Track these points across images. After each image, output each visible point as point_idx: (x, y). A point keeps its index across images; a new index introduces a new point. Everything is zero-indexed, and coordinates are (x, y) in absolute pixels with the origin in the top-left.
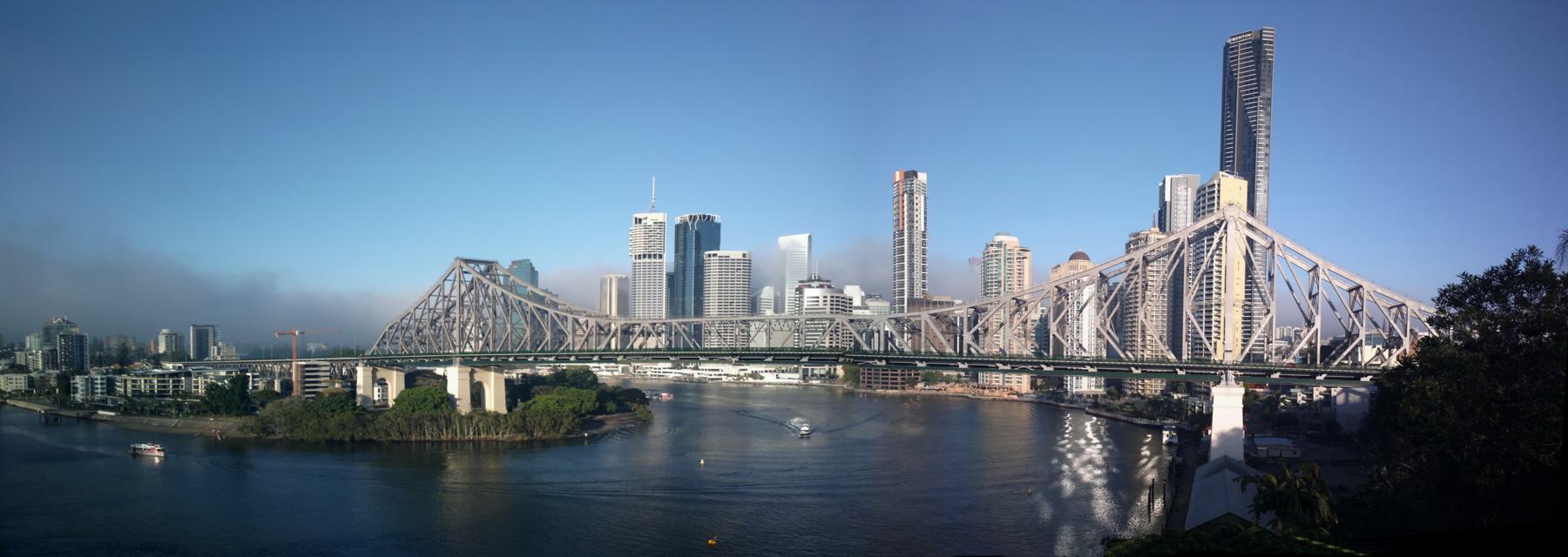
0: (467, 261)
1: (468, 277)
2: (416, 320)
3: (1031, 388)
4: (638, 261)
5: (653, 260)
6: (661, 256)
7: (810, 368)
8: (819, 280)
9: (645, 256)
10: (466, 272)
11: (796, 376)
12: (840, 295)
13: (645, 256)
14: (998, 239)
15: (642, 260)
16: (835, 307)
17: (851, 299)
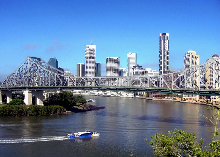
0: (32, 58)
1: (32, 63)
2: (15, 76)
3: (200, 99)
4: (87, 59)
5: (92, 59)
6: (94, 58)
7: (136, 92)
8: (138, 66)
9: (89, 58)
10: (31, 61)
11: (133, 94)
12: (145, 71)
13: (89, 58)
14: (189, 52)
15: (89, 59)
16: (143, 74)
17: (147, 72)
